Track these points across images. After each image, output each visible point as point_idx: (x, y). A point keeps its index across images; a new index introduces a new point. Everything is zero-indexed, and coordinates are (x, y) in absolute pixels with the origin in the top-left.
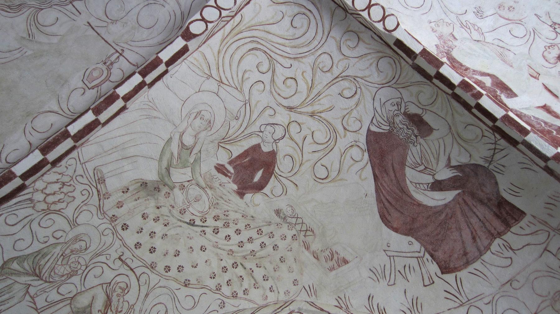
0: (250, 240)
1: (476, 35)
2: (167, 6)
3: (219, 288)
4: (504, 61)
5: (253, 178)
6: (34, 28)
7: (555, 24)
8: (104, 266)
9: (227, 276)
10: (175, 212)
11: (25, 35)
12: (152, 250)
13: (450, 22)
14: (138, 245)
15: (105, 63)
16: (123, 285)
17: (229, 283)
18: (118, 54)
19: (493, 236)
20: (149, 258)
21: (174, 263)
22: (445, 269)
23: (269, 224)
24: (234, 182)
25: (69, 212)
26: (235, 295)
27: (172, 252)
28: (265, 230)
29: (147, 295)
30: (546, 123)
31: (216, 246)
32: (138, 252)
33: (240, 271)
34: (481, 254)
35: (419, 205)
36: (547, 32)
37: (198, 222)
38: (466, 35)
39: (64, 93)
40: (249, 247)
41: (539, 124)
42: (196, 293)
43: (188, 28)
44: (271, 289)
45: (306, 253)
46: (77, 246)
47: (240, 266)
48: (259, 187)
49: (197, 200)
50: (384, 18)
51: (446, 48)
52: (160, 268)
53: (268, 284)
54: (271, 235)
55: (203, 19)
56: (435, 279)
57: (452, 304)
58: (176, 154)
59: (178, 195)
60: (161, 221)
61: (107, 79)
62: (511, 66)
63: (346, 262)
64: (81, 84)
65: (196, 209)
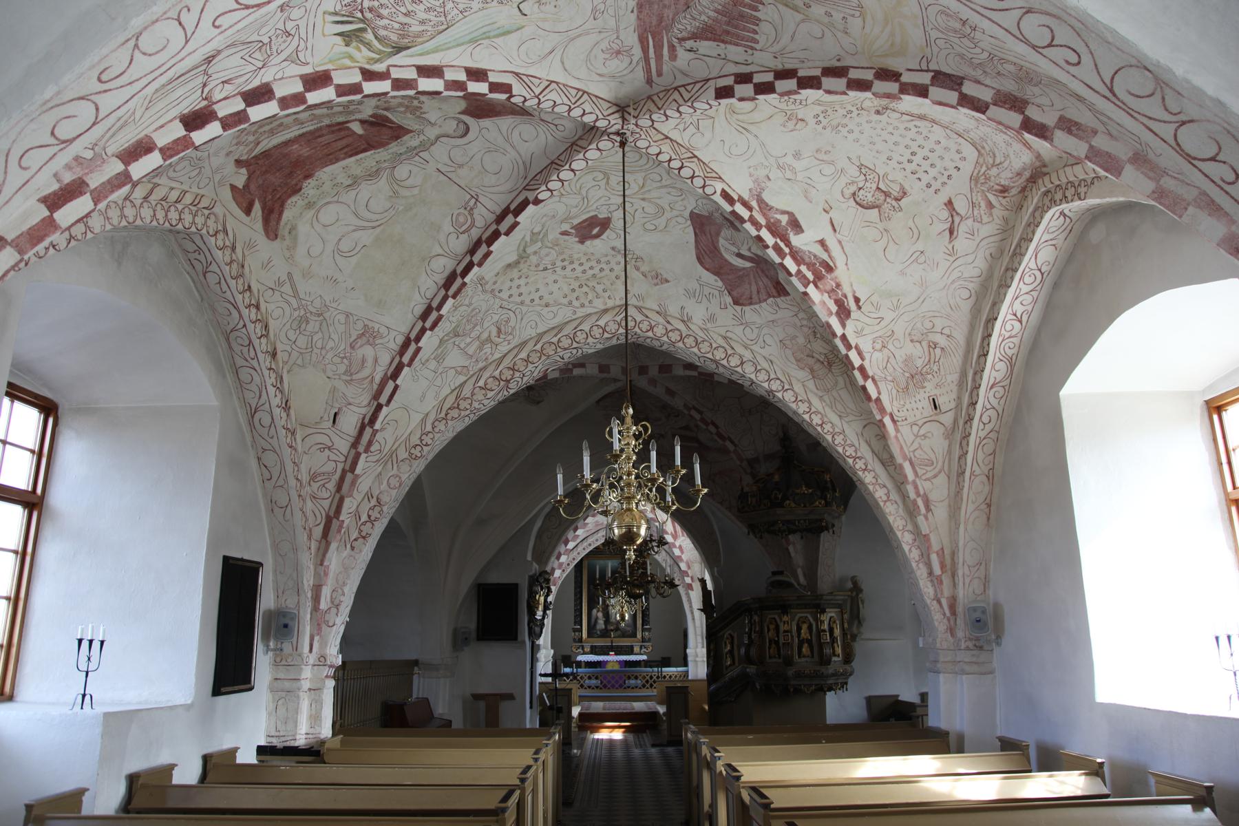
0: (591, 268)
1: (789, 175)
2: (508, 155)
3: (570, 303)
4: (806, 197)
5: (591, 232)
6: (395, 185)
7: (862, 165)
8: (493, 315)
9: (575, 295)
10: (533, 268)
11: (392, 194)
12: (520, 295)
13: (768, 164)
14: (511, 296)
15: (465, 208)
16: (506, 319)
17: (577, 299)
18: (473, 200)
19: (770, 296)
20: (519, 300)
21: (536, 296)
22: (736, 302)
23: (606, 256)
24: (576, 237)
25: (467, 302)
26: (583, 306)
27: (533, 290)
28: (603, 260)
29: (522, 319)
30: (815, 256)
31: (565, 277)
32: (511, 299)
33: (585, 289)
34: (760, 302)
35: (726, 261)
36: (853, 171)
37: (549, 267)
38: (780, 175)
39: (442, 238)
40: (591, 272)
41: (810, 258)
42: (554, 309)
43: (536, 197)
44: (609, 297)
45: (636, 272)
46: (474, 313)
47: (585, 286)
48: (598, 236)
49: (547, 255)
50: (704, 187)
51: (759, 190)
52: (527, 302)
53: (607, 295)
54: (608, 262)
55: (549, 190)
56: (729, 306)
57: (736, 323)
58: (529, 240)
59: (534, 259)
60: (523, 277)
61: (473, 225)
62: (811, 202)
63: (667, 281)
64: (452, 230)
65: (547, 261)
